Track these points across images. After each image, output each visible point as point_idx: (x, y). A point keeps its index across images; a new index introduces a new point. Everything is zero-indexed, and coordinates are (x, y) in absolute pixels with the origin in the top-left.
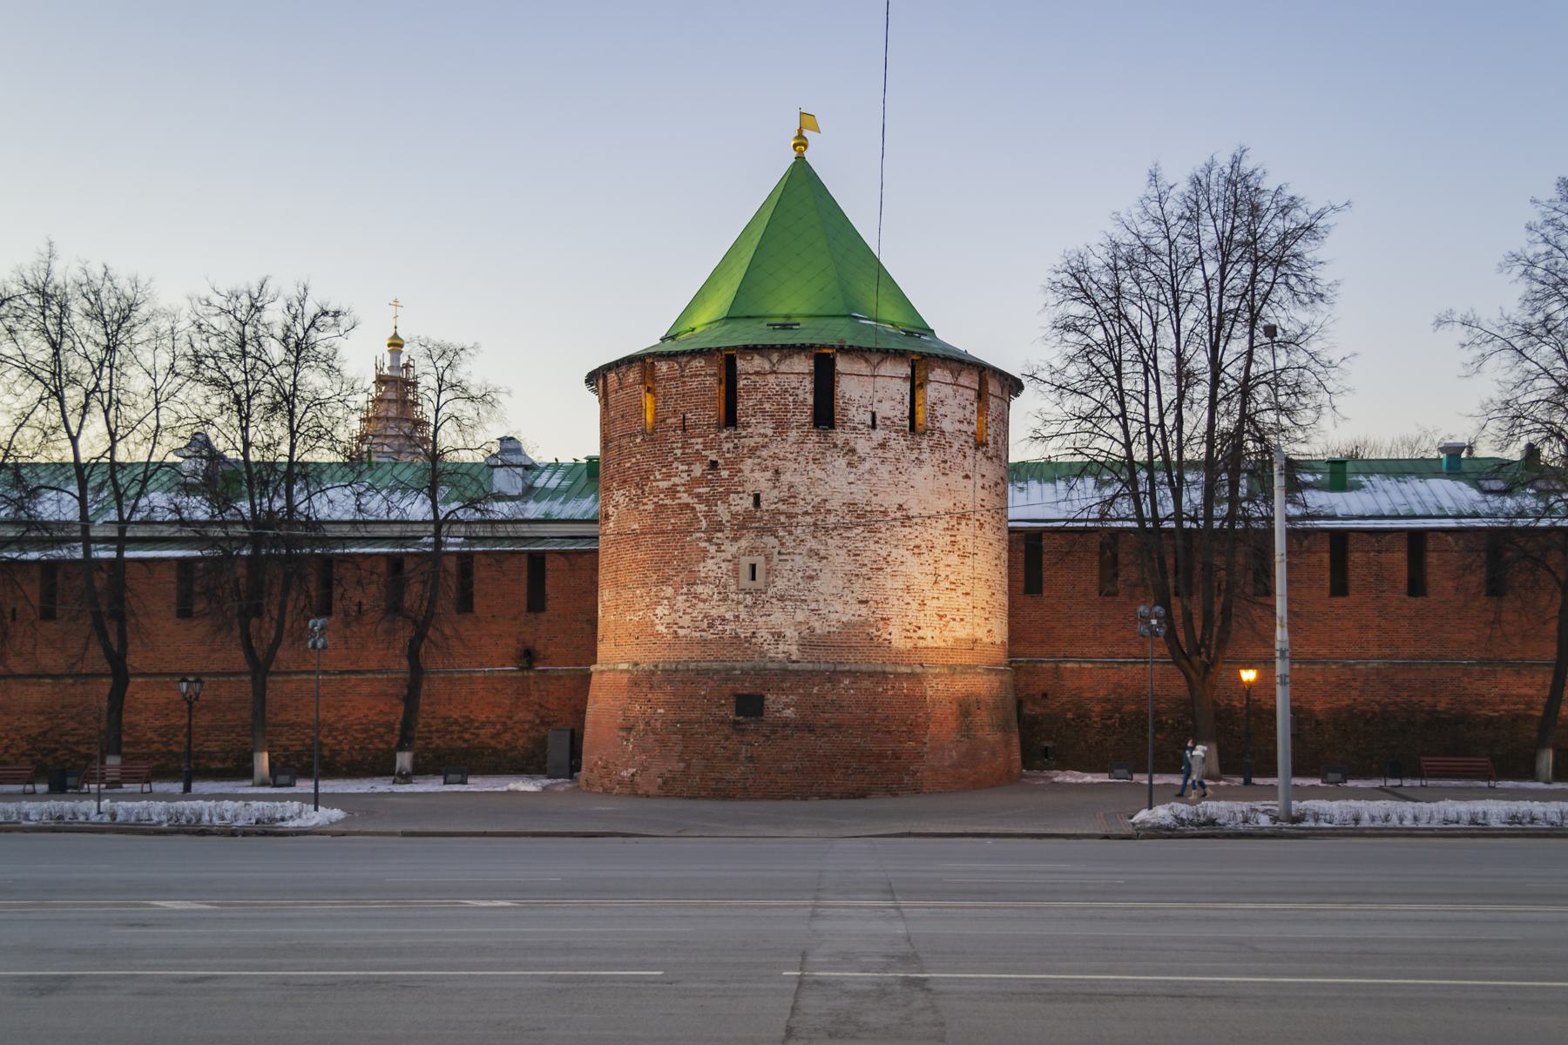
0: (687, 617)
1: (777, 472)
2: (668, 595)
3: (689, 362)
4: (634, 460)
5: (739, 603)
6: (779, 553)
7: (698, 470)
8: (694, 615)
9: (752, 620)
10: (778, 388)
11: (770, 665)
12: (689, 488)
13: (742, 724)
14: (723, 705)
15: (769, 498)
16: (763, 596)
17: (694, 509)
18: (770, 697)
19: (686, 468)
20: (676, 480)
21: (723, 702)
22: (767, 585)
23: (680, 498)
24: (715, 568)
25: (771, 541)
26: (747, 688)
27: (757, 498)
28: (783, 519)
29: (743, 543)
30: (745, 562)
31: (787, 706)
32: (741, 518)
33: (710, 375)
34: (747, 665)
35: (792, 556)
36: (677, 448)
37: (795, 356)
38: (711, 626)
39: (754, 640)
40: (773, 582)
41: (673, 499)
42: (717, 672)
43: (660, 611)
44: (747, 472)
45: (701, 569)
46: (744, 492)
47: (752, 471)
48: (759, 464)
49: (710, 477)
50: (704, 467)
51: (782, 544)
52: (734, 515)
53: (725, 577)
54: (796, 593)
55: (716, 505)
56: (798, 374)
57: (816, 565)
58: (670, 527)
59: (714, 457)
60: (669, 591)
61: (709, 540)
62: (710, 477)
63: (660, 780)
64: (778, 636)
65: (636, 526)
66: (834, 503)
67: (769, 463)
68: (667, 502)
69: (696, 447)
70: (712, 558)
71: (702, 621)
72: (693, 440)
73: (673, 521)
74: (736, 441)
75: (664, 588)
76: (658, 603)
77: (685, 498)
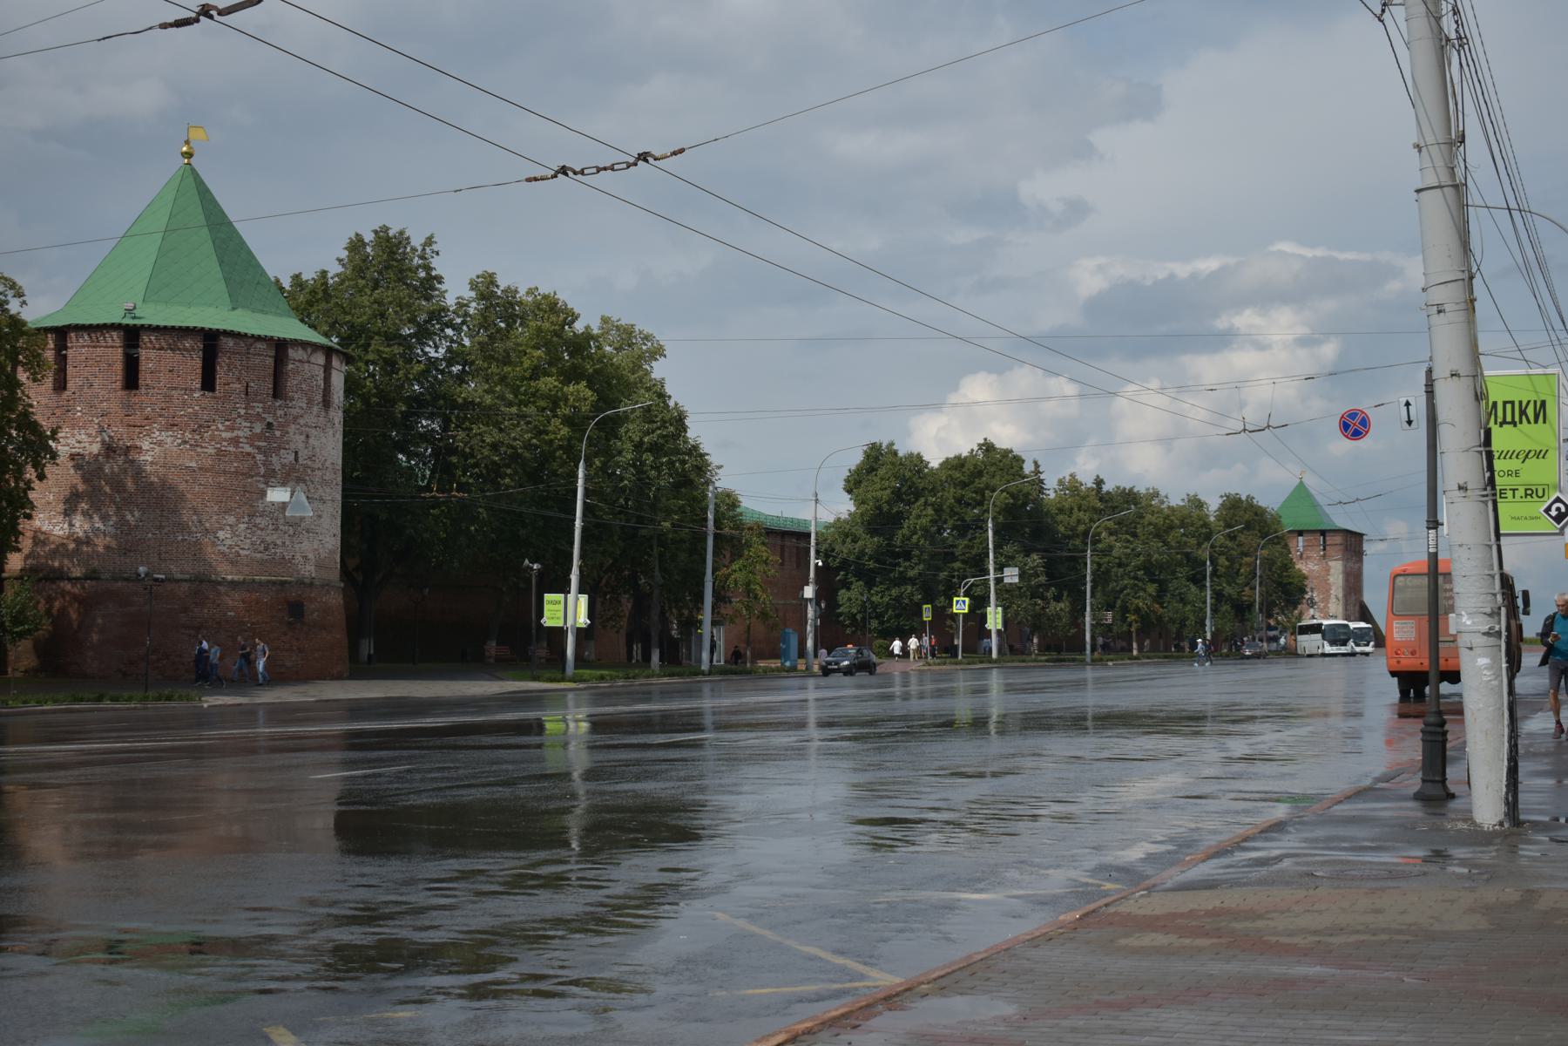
0: (248, 541)
5: (285, 533)
7: (258, 428)
12: (251, 440)
15: (303, 454)
17: (254, 457)
19: (249, 425)
20: (240, 433)
27: (296, 453)
38: (266, 549)
47: (295, 434)
52: (284, 466)
57: (322, 507)
59: (270, 420)
60: (231, 520)
64: (305, 557)
68: (231, 449)
73: (236, 465)
77: (248, 449)
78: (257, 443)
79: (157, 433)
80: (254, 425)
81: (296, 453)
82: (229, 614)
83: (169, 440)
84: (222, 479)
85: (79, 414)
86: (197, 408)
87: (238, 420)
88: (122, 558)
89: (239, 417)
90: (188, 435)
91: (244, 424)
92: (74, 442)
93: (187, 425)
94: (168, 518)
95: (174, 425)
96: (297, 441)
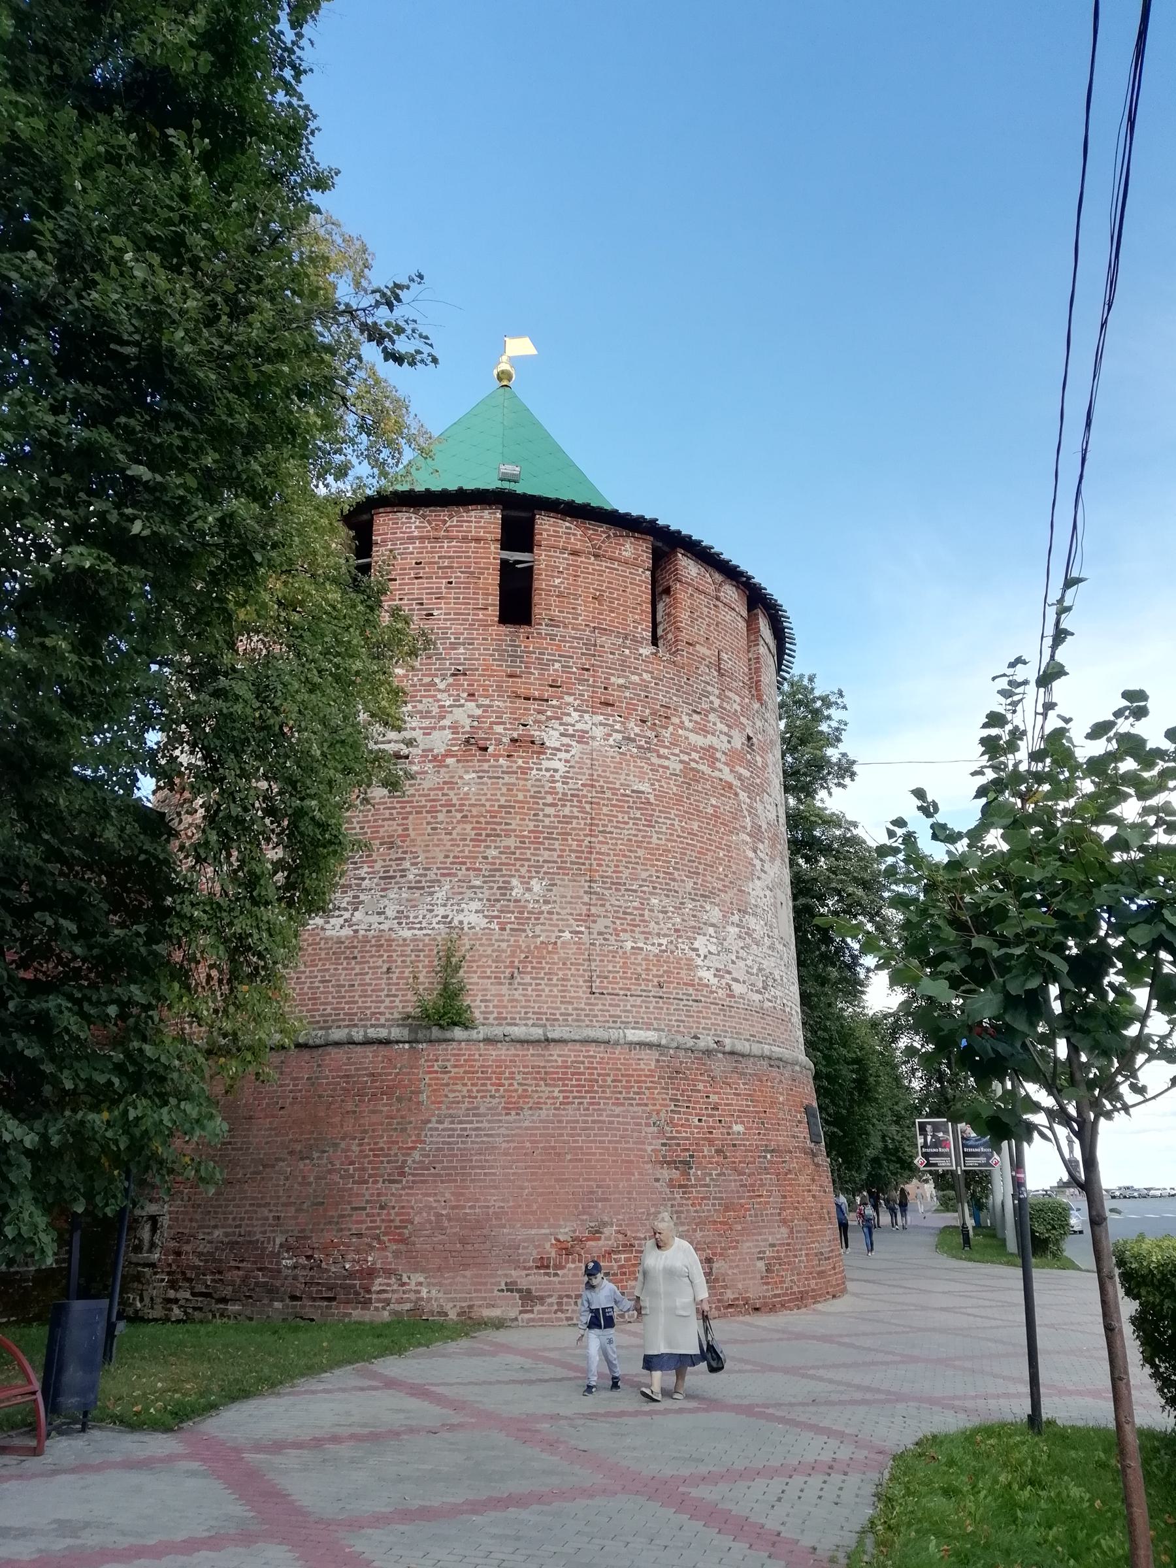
0: (741, 964)
2: (714, 921)
4: (635, 678)
23: (720, 770)
58: (710, 810)
60: (715, 914)
63: (761, 1265)
65: (645, 787)
77: (727, 775)
79: (575, 715)
83: (599, 732)
88: (504, 989)
90: (634, 728)
93: (631, 708)
94: (602, 897)
95: (607, 704)
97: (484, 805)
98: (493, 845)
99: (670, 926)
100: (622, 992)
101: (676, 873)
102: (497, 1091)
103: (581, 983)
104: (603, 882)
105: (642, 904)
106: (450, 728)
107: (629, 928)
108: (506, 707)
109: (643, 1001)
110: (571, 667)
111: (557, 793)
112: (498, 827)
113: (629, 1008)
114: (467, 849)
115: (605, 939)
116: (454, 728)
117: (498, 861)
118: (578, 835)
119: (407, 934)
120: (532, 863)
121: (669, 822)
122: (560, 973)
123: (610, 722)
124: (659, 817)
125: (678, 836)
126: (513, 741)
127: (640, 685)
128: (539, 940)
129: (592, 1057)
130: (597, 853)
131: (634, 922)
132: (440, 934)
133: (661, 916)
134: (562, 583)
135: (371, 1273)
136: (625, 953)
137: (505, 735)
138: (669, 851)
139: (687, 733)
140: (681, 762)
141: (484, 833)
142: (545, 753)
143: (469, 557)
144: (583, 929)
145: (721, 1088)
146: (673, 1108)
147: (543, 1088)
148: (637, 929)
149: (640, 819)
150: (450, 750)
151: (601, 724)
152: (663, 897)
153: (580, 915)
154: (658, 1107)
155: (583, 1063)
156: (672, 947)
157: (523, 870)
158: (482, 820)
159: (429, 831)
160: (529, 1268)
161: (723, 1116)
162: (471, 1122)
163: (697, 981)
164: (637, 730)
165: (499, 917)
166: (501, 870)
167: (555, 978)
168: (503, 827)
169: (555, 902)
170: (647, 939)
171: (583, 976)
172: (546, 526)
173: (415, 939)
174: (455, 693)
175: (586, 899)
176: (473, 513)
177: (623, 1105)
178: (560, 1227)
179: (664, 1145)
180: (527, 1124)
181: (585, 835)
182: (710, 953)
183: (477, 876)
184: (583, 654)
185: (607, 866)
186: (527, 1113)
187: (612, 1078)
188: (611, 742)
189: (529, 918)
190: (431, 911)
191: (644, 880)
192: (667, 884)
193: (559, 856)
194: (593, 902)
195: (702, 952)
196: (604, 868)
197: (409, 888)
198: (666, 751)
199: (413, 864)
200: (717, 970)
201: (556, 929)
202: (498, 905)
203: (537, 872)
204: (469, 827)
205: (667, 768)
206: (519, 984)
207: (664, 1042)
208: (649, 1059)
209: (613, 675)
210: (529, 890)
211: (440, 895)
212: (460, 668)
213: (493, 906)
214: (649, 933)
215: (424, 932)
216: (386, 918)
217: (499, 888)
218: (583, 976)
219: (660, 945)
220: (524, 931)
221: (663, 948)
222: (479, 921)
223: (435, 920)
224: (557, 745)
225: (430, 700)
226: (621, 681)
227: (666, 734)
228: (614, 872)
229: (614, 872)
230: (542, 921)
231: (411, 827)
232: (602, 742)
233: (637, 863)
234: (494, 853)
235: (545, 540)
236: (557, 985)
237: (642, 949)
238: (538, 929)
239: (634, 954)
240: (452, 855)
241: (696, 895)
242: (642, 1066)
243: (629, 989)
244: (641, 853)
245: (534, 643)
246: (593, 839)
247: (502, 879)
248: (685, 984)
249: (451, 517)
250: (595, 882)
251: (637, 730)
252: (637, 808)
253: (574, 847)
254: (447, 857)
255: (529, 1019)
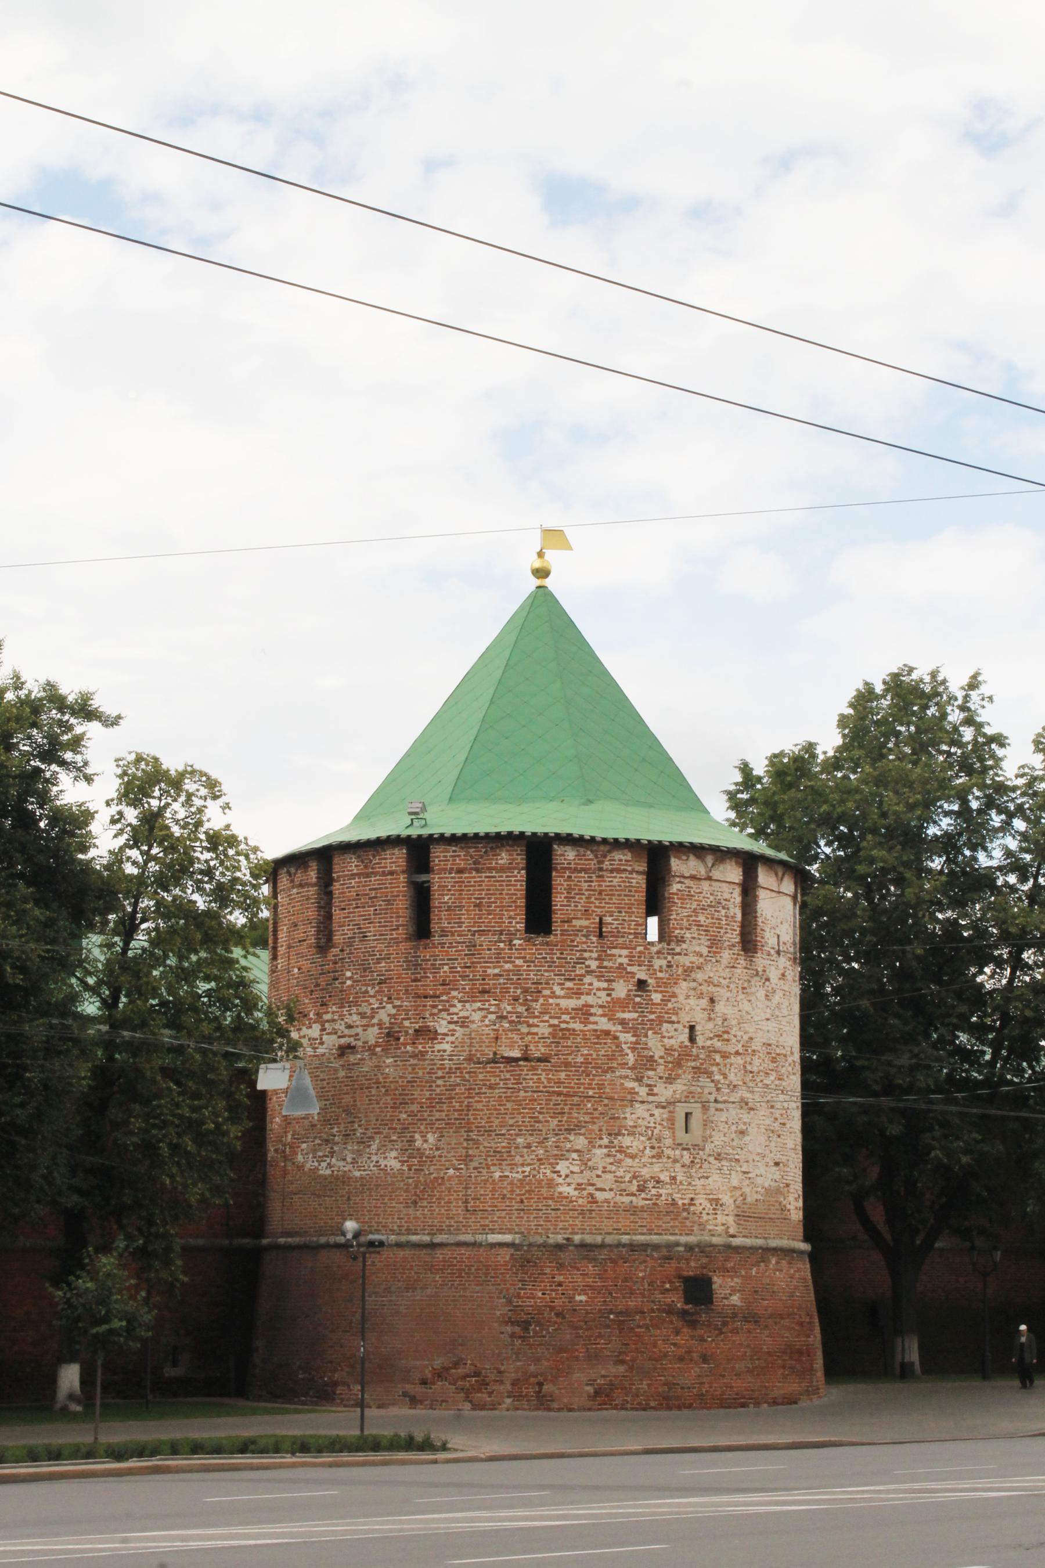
0: (610, 1176)
1: (712, 1001)
3: (610, 851)
4: (508, 966)
5: (675, 1161)
6: (716, 1101)
7: (621, 990)
8: (618, 1174)
9: (690, 1184)
10: (712, 898)
11: (715, 1240)
12: (610, 1009)
13: (692, 1314)
14: (667, 1290)
15: (705, 1030)
16: (701, 1153)
17: (616, 1038)
18: (717, 1281)
20: (590, 999)
21: (668, 1286)
22: (705, 1139)
23: (596, 1023)
24: (646, 1115)
25: (704, 1080)
26: (691, 1269)
27: (692, 1028)
28: (718, 1058)
29: (679, 1087)
30: (680, 1111)
31: (733, 1291)
32: (676, 1054)
33: (638, 872)
34: (692, 1239)
35: (727, 1105)
36: (591, 958)
37: (728, 861)
38: (642, 1189)
39: (692, 1208)
40: (711, 1137)
41: (586, 1022)
42: (656, 1247)
43: (562, 1167)
44: (681, 998)
45: (628, 1115)
46: (678, 1022)
47: (688, 997)
48: (694, 989)
49: (638, 999)
50: (630, 987)
51: (718, 1089)
52: (669, 1050)
53: (659, 1127)
54: (731, 1151)
55: (646, 1036)
56: (730, 883)
57: (746, 1118)
58: (580, 1059)
59: (642, 975)
60: (580, 1142)
61: (639, 1080)
62: (638, 999)
63: (590, 1389)
64: (716, 1202)
66: (756, 1045)
67: (704, 988)
68: (577, 1026)
69: (620, 960)
70: (642, 1102)
71: (630, 1182)
72: (614, 951)
74: (669, 958)
75: (572, 1138)
76: (562, 1157)
77: (604, 1024)
78: (621, 1015)
79: (459, 1006)
80: (614, 985)
81: (692, 1028)
82: (578, 1298)
83: (477, 1016)
84: (563, 1075)
85: (349, 982)
86: (519, 962)
87: (588, 979)
88: (411, 1211)
89: (589, 972)
91: (597, 984)
92: (343, 1028)
94: (477, 1142)
95: (484, 992)
96: (693, 1009)
97: (397, 1082)
98: (403, 1111)
99: (533, 1157)
100: (490, 1209)
101: (541, 1116)
102: (402, 1277)
103: (460, 1204)
104: (478, 1131)
105: (509, 1143)
106: (378, 1024)
107: (498, 1162)
108: (411, 1006)
109: (507, 1214)
110: (456, 968)
111: (445, 1068)
112: (406, 1097)
113: (495, 1219)
114: (388, 1114)
115: (479, 1172)
116: (380, 1025)
117: (407, 1122)
118: (460, 1098)
119: (357, 1174)
120: (428, 1122)
121: (535, 1077)
122: (447, 1198)
123: (487, 1006)
124: (527, 1075)
125: (545, 1087)
126: (416, 1031)
127: (513, 971)
128: (432, 1177)
129: (462, 1254)
130: (474, 1110)
131: (501, 1157)
132: (374, 1174)
133: (525, 1150)
134: (450, 899)
135: (336, 1384)
136: (494, 1181)
137: (409, 1028)
138: (535, 1100)
139: (558, 1001)
140: (550, 1026)
141: (398, 1102)
142: (437, 1039)
143: (386, 888)
144: (462, 1166)
145: (568, 1270)
146: (520, 1286)
147: (430, 1275)
148: (505, 1162)
149: (510, 1079)
150: (377, 1042)
151: (480, 1009)
152: (528, 1136)
153: (461, 1156)
154: (508, 1286)
155: (456, 1258)
156: (535, 1173)
157: (422, 1128)
158: (397, 1092)
159: (367, 1102)
160: (416, 1384)
161: (567, 1290)
162: (387, 1296)
163: (556, 1195)
164: (509, 1008)
165: (408, 1161)
166: (408, 1128)
167: (443, 1202)
168: (410, 1097)
169: (443, 1149)
170: (513, 1168)
171: (461, 1199)
172: (439, 855)
173: (362, 1178)
174: (380, 998)
175: (465, 1144)
176: (388, 852)
177: (482, 1285)
178: (434, 1360)
179: (510, 1310)
180: (418, 1298)
181: (465, 1098)
182: (572, 1172)
183: (394, 1133)
184: (466, 955)
185: (481, 1118)
186: (419, 1291)
187: (475, 1267)
188: (487, 1022)
189: (426, 1161)
190: (369, 1158)
191: (511, 1126)
192: (531, 1126)
193: (446, 1115)
194: (471, 1146)
195: (563, 1173)
196: (479, 1120)
197: (358, 1143)
198: (535, 1020)
199: (360, 1126)
200: (578, 1184)
201: (443, 1168)
202: (407, 1153)
203: (432, 1128)
204: (389, 1098)
205: (537, 1034)
206: (420, 1207)
207: (517, 1241)
208: (506, 1254)
209: (489, 967)
210: (426, 1141)
211: (374, 1147)
212: (383, 978)
213: (404, 1154)
214: (515, 1164)
215: (367, 1172)
216: (347, 1163)
217: (407, 1141)
218: (461, 1199)
219: (523, 1172)
220: (423, 1170)
221: (527, 1174)
222: (395, 1164)
223: (372, 1165)
224: (445, 1031)
225: (366, 1004)
226: (497, 971)
227: (537, 1006)
228: (487, 1122)
229: (487, 1122)
230: (434, 1162)
231: (358, 1099)
232: (480, 1024)
233: (506, 1114)
234: (404, 1116)
235: (437, 865)
236: (443, 1207)
237: (508, 1177)
238: (432, 1168)
239: (501, 1181)
240: (380, 1118)
241: (560, 1130)
242: (499, 1259)
243: (496, 1206)
244: (509, 1105)
245: (429, 952)
246: (470, 1100)
247: (408, 1135)
248: (545, 1198)
249: (374, 856)
250: (472, 1131)
251: (509, 1008)
252: (507, 1071)
253: (457, 1108)
254: (377, 1120)
255: (425, 1230)
